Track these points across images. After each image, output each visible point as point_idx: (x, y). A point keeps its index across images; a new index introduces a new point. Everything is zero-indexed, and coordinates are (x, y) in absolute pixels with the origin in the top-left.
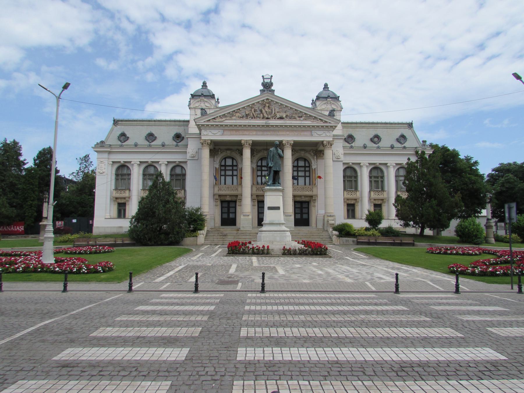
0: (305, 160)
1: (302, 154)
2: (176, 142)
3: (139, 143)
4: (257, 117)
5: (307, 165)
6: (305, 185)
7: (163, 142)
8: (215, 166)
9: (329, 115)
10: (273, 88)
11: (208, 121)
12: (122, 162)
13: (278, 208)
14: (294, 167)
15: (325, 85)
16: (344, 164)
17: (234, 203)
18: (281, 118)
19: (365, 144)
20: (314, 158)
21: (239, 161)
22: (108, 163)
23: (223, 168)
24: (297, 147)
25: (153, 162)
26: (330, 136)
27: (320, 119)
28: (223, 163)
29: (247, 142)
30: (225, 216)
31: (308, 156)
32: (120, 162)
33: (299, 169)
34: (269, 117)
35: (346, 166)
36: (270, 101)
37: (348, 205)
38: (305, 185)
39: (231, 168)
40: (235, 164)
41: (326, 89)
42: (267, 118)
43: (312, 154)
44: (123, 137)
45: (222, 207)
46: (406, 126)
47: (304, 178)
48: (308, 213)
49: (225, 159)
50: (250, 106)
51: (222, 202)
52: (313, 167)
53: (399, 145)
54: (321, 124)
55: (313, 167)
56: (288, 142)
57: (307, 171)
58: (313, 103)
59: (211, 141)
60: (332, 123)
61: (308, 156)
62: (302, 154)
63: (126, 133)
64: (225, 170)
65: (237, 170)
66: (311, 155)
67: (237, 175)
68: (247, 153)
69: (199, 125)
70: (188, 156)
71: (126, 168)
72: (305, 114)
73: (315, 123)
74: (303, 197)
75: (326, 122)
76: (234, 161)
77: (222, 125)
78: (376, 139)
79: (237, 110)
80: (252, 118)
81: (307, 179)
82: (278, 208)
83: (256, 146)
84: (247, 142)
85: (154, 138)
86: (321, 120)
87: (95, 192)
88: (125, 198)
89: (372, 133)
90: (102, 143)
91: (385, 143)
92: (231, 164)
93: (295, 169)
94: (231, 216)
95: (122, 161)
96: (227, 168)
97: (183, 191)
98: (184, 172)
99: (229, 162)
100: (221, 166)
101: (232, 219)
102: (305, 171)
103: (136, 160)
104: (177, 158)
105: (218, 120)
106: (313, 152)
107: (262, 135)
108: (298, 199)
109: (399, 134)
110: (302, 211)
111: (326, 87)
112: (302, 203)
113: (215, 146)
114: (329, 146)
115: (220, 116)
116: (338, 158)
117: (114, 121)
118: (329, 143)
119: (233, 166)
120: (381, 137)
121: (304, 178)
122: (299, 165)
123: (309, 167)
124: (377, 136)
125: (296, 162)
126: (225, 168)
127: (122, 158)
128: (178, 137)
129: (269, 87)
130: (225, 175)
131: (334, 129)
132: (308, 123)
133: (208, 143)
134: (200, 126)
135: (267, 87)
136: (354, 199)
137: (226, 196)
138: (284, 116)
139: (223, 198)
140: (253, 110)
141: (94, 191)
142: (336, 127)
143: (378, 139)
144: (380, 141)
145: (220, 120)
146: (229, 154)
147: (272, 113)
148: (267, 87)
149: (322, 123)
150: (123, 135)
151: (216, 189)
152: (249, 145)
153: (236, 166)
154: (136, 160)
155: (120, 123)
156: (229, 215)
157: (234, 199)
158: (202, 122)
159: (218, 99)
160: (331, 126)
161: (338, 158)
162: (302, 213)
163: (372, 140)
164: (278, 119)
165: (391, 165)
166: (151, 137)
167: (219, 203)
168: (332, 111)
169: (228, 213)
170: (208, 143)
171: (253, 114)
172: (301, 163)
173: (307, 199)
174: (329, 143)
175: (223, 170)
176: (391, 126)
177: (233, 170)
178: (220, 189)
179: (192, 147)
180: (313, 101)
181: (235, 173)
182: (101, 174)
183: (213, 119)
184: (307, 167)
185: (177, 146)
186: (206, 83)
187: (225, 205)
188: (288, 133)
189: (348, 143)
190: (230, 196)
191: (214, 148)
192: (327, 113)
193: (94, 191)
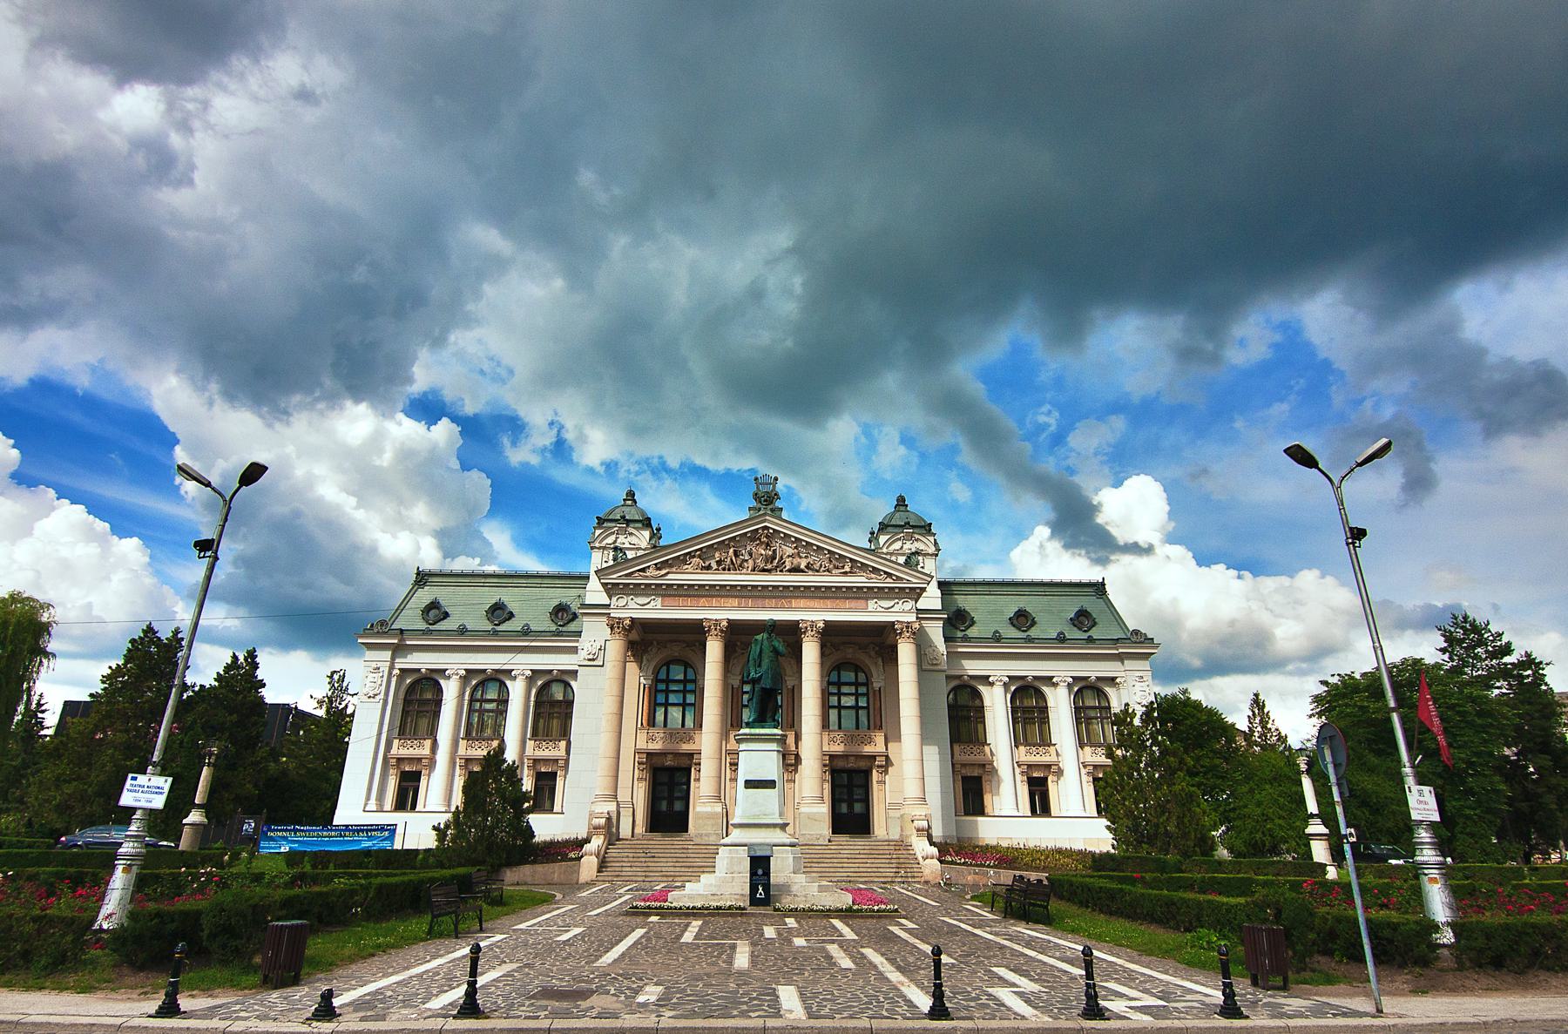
0: (857, 669)
1: (849, 653)
2: (556, 624)
3: (469, 628)
4: (741, 566)
6: (857, 728)
9: (907, 564)
10: (778, 504)
11: (626, 575)
12: (423, 670)
13: (770, 784)
14: (829, 683)
15: (897, 500)
16: (949, 678)
18: (796, 570)
19: (997, 632)
21: (700, 670)
22: (390, 673)
23: (662, 686)
24: (831, 635)
25: (497, 671)
26: (909, 611)
27: (885, 573)
28: (663, 676)
31: (863, 658)
32: (419, 670)
33: (845, 689)
34: (769, 567)
35: (954, 683)
37: (965, 779)
38: (857, 728)
39: (681, 687)
40: (691, 676)
41: (902, 508)
42: (764, 570)
43: (873, 653)
44: (434, 611)
47: (854, 712)
48: (866, 800)
49: (668, 664)
52: (876, 686)
54: (889, 583)
55: (875, 685)
57: (863, 695)
58: (873, 537)
59: (633, 620)
61: (863, 658)
62: (849, 653)
64: (667, 692)
65: (693, 692)
66: (870, 656)
67: (693, 705)
68: (714, 650)
69: (607, 584)
70: (583, 654)
71: (432, 682)
72: (851, 560)
74: (852, 758)
76: (690, 671)
78: (1022, 619)
80: (729, 570)
82: (750, 784)
83: (737, 635)
86: (890, 575)
87: (347, 743)
88: (419, 760)
89: (1011, 605)
91: (1047, 627)
92: (681, 677)
93: (833, 690)
95: (423, 668)
96: (673, 687)
97: (563, 744)
99: (677, 673)
102: (857, 695)
105: (652, 572)
107: (753, 608)
108: (840, 764)
110: (850, 794)
111: (901, 502)
112: (851, 772)
113: (645, 633)
114: (908, 634)
115: (656, 564)
116: (933, 665)
117: (418, 574)
118: (908, 627)
119: (685, 681)
121: (854, 712)
122: (843, 679)
123: (866, 684)
125: (835, 673)
126: (667, 687)
127: (422, 661)
128: (563, 614)
129: (771, 503)
130: (666, 705)
131: (919, 595)
132: (859, 580)
133: (624, 627)
136: (979, 765)
138: (802, 567)
141: (347, 740)
142: (923, 590)
146: (677, 654)
150: (434, 605)
151: (642, 736)
152: (722, 631)
153: (694, 681)
157: (684, 762)
158: (614, 578)
159: (658, 530)
161: (933, 665)
164: (789, 571)
166: (498, 612)
170: (624, 627)
171: (731, 559)
172: (848, 676)
173: (862, 764)
175: (661, 691)
177: (685, 692)
179: (594, 634)
180: (872, 533)
181: (690, 699)
182: (372, 700)
183: (639, 570)
184: (862, 684)
186: (634, 494)
187: (664, 778)
191: (642, 640)
192: (902, 560)
193: (347, 740)
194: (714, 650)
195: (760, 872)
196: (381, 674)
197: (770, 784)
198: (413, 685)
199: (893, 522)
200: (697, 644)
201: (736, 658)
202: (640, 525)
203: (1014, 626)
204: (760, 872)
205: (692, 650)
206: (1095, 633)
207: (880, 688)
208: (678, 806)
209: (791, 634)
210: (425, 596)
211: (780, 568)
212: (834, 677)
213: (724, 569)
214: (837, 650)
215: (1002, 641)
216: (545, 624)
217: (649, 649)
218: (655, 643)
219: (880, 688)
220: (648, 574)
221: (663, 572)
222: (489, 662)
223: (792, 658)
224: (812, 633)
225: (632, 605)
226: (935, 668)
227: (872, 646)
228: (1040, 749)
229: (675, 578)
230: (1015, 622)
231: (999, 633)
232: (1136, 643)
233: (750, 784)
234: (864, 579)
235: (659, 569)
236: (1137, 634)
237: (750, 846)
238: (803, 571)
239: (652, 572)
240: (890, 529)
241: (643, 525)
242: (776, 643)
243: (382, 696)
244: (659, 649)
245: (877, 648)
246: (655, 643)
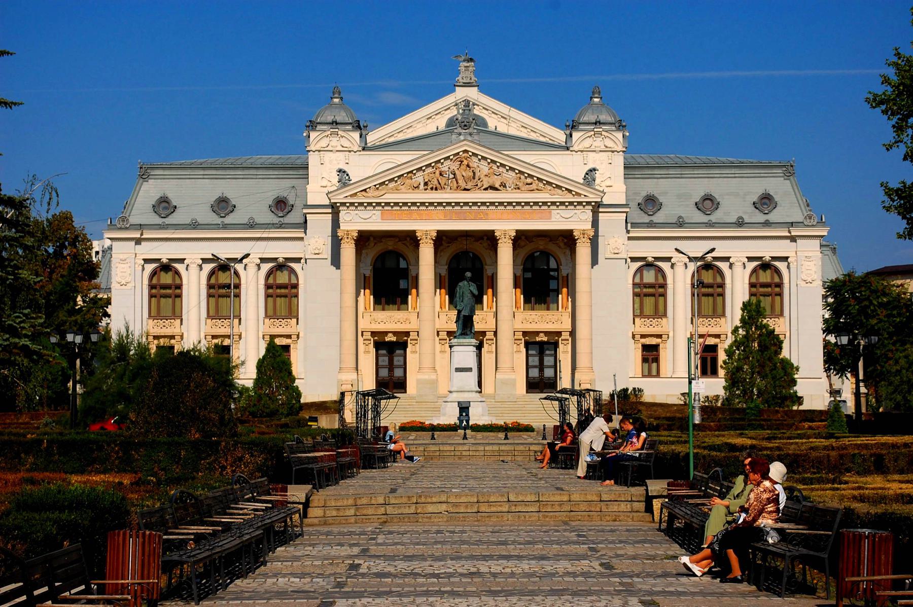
7: (252, 218)
8: (362, 271)
11: (351, 196)
13: (470, 370)
18: (493, 188)
21: (412, 261)
27: (567, 189)
29: (427, 235)
31: (552, 247)
36: (471, 154)
37: (646, 348)
42: (465, 189)
43: (562, 245)
45: (377, 357)
50: (433, 165)
54: (569, 198)
56: (505, 233)
60: (591, 196)
61: (552, 247)
63: (171, 196)
66: (560, 247)
68: (427, 253)
72: (538, 178)
73: (558, 197)
75: (578, 194)
77: (379, 204)
79: (408, 173)
80: (436, 189)
84: (427, 235)
85: (230, 208)
86: (570, 191)
90: (123, 221)
91: (729, 210)
104: (281, 251)
105: (371, 193)
106: (563, 240)
109: (761, 192)
115: (375, 186)
118: (584, 234)
123: (557, 270)
124: (708, 198)
127: (165, 252)
134: (338, 205)
135: (465, 126)
137: (386, 333)
138: (497, 186)
140: (438, 172)
143: (713, 204)
145: (377, 193)
146: (390, 248)
148: (465, 126)
149: (571, 196)
160: (588, 203)
162: (541, 367)
164: (484, 189)
165: (737, 261)
168: (591, 170)
169: (391, 367)
174: (584, 234)
183: (361, 191)
194: (427, 253)
195: (464, 414)
196: (129, 265)
197: (470, 370)
200: (408, 239)
201: (441, 251)
202: (349, 127)
203: (699, 209)
204: (464, 414)
205: (403, 244)
206: (773, 217)
207: (568, 274)
208: (398, 373)
213: (432, 189)
214: (530, 242)
215: (686, 225)
217: (367, 244)
218: (372, 239)
219: (568, 274)
220: (369, 195)
223: (491, 250)
224: (505, 240)
226: (616, 256)
227: (560, 238)
228: (712, 321)
230: (700, 206)
231: (683, 219)
232: (808, 226)
233: (458, 370)
234: (547, 195)
236: (810, 218)
237: (459, 403)
238: (497, 189)
240: (581, 127)
241: (353, 127)
242: (472, 288)
244: (375, 244)
245: (566, 241)
246: (372, 239)
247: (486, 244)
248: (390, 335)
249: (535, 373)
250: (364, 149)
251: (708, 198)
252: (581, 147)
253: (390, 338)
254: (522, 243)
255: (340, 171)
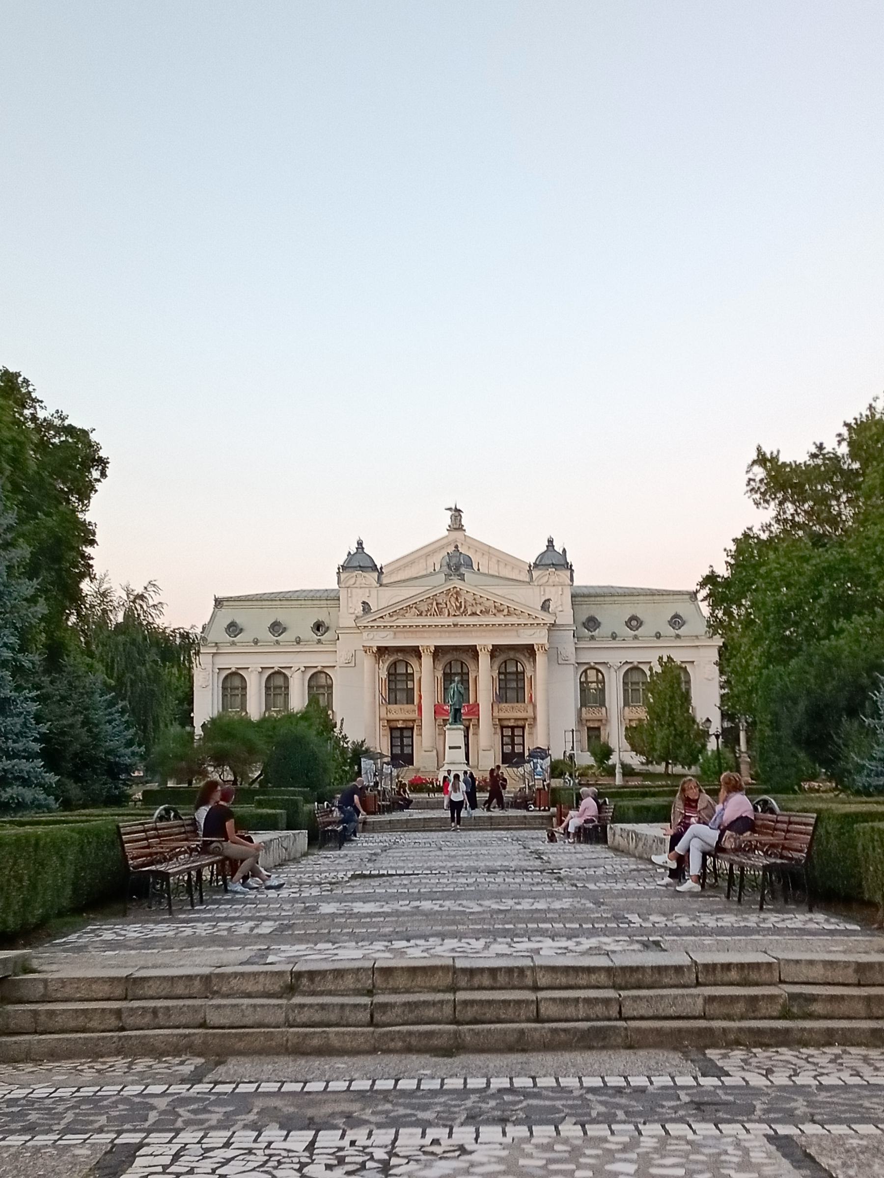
5: (520, 669)
17: (410, 731)
18: (474, 614)
20: (529, 661)
24: (496, 651)
30: (397, 751)
34: (458, 613)
43: (527, 655)
44: (233, 628)
46: (688, 597)
51: (392, 729)
53: (671, 631)
81: (520, 691)
83: (438, 652)
94: (407, 750)
98: (329, 681)
100: (389, 674)
101: (408, 754)
102: (517, 681)
103: (255, 666)
104: (319, 661)
105: (387, 618)
110: (513, 740)
117: (216, 600)
120: (642, 619)
139: (393, 724)
144: (640, 626)
147: (461, 606)
151: (383, 710)
154: (255, 666)
155: (225, 603)
156: (402, 750)
163: (628, 624)
166: (277, 628)
167: (388, 732)
168: (545, 601)
173: (520, 723)
176: (661, 597)
178: (388, 711)
185: (319, 641)
187: (397, 734)
188: (484, 634)
189: (589, 630)
190: (404, 721)
198: (226, 678)
199: (543, 562)
208: (407, 750)
209: (473, 651)
210: (226, 616)
211: (464, 613)
212: (503, 670)
216: (309, 634)
221: (394, 618)
222: (276, 662)
225: (376, 638)
229: (401, 622)
235: (391, 616)
239: (387, 618)
243: (210, 687)
247: (471, 654)
248: (401, 722)
249: (508, 749)
250: (381, 585)
251: (633, 618)
252: (540, 583)
253: (400, 725)
254: (497, 654)
255: (364, 603)
